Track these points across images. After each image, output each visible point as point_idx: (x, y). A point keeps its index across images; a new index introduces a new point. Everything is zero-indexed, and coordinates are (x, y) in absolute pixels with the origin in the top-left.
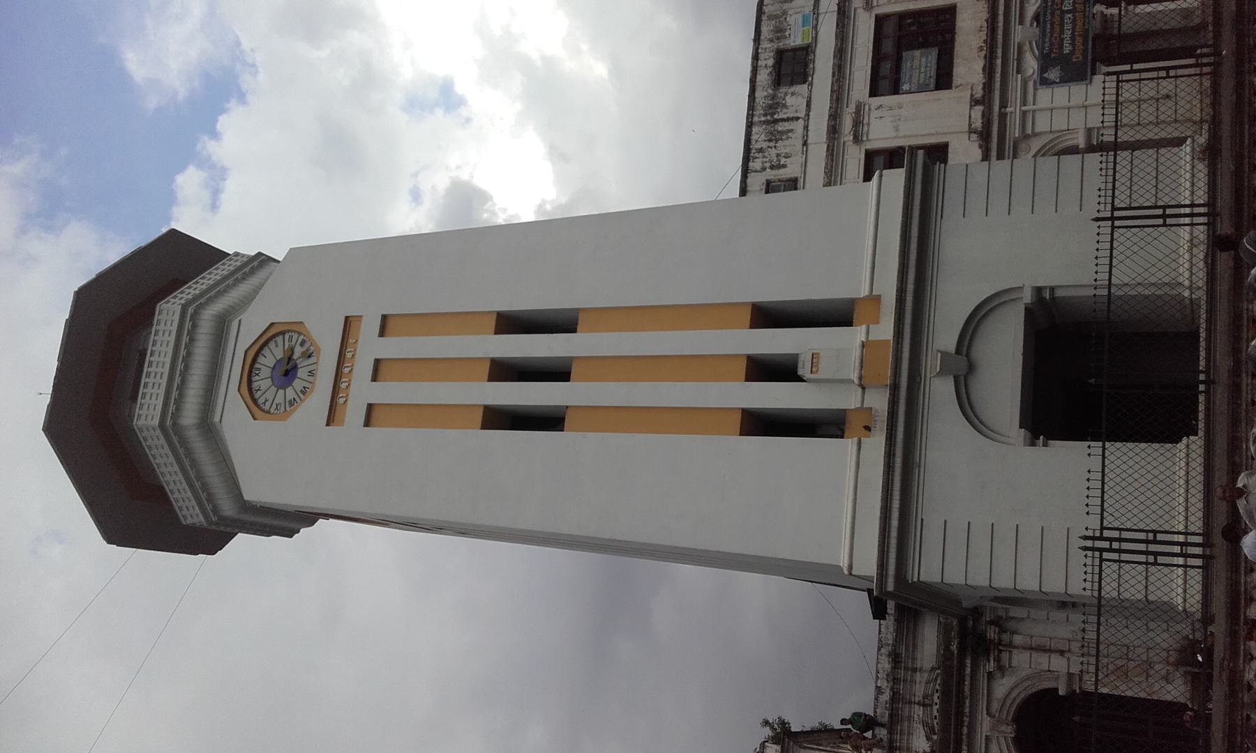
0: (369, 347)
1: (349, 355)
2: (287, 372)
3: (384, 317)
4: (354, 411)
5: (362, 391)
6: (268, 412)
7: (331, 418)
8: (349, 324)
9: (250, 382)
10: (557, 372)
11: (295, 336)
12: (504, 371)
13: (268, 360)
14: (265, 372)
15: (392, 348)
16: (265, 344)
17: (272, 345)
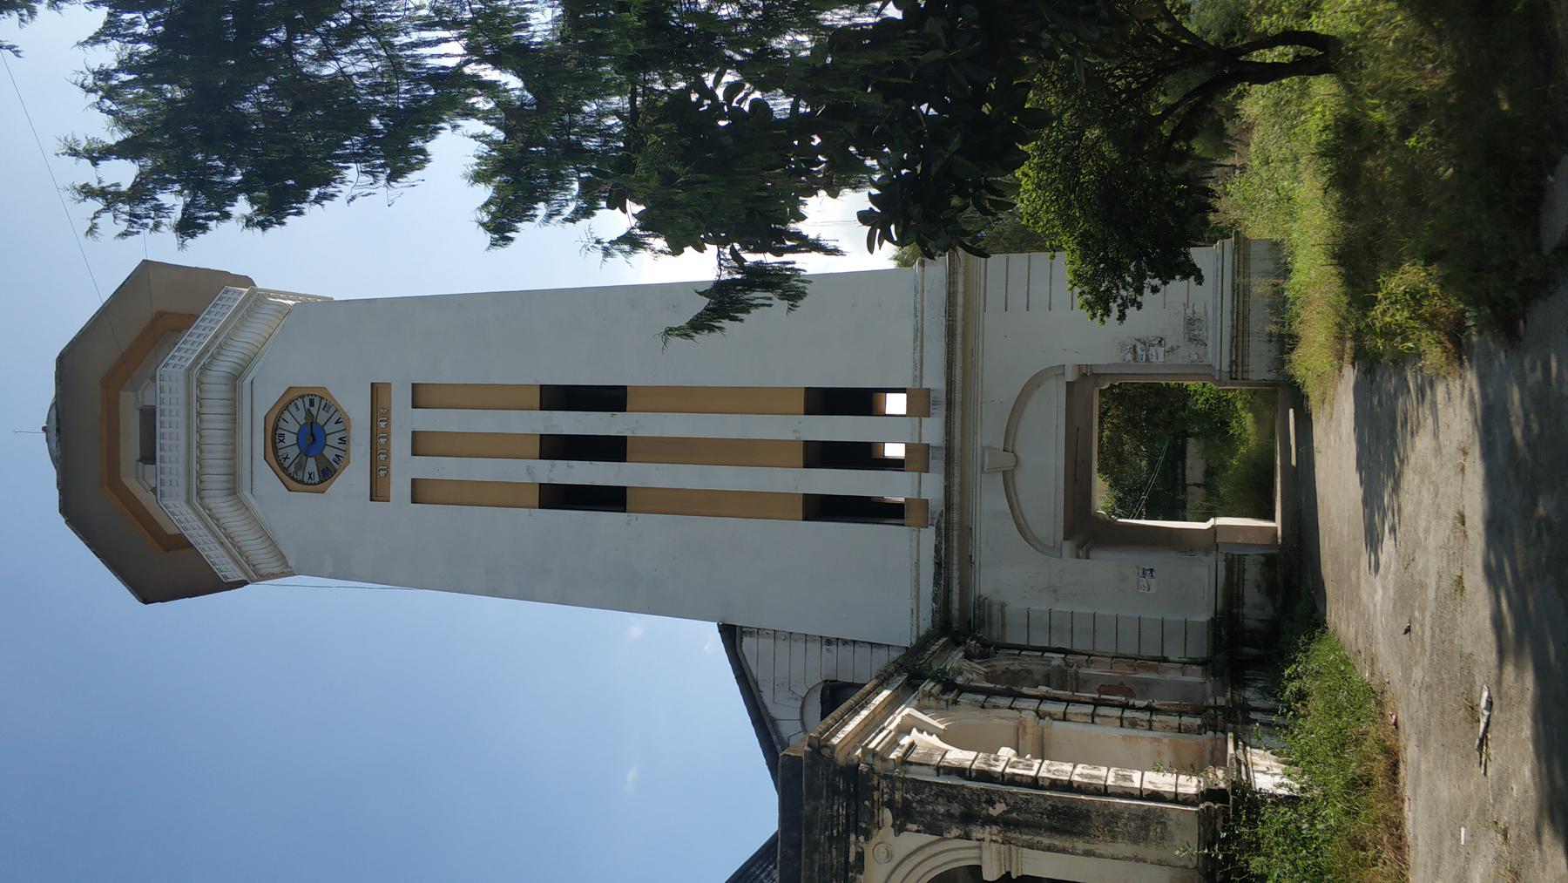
0: (405, 420)
1: (383, 424)
2: (312, 437)
3: (415, 387)
4: (399, 487)
5: (404, 468)
6: (301, 482)
7: (378, 492)
8: (378, 392)
9: (275, 450)
10: (612, 449)
11: (317, 401)
12: (558, 447)
13: (292, 424)
14: (290, 439)
15: (428, 420)
16: (286, 408)
17: (292, 408)
